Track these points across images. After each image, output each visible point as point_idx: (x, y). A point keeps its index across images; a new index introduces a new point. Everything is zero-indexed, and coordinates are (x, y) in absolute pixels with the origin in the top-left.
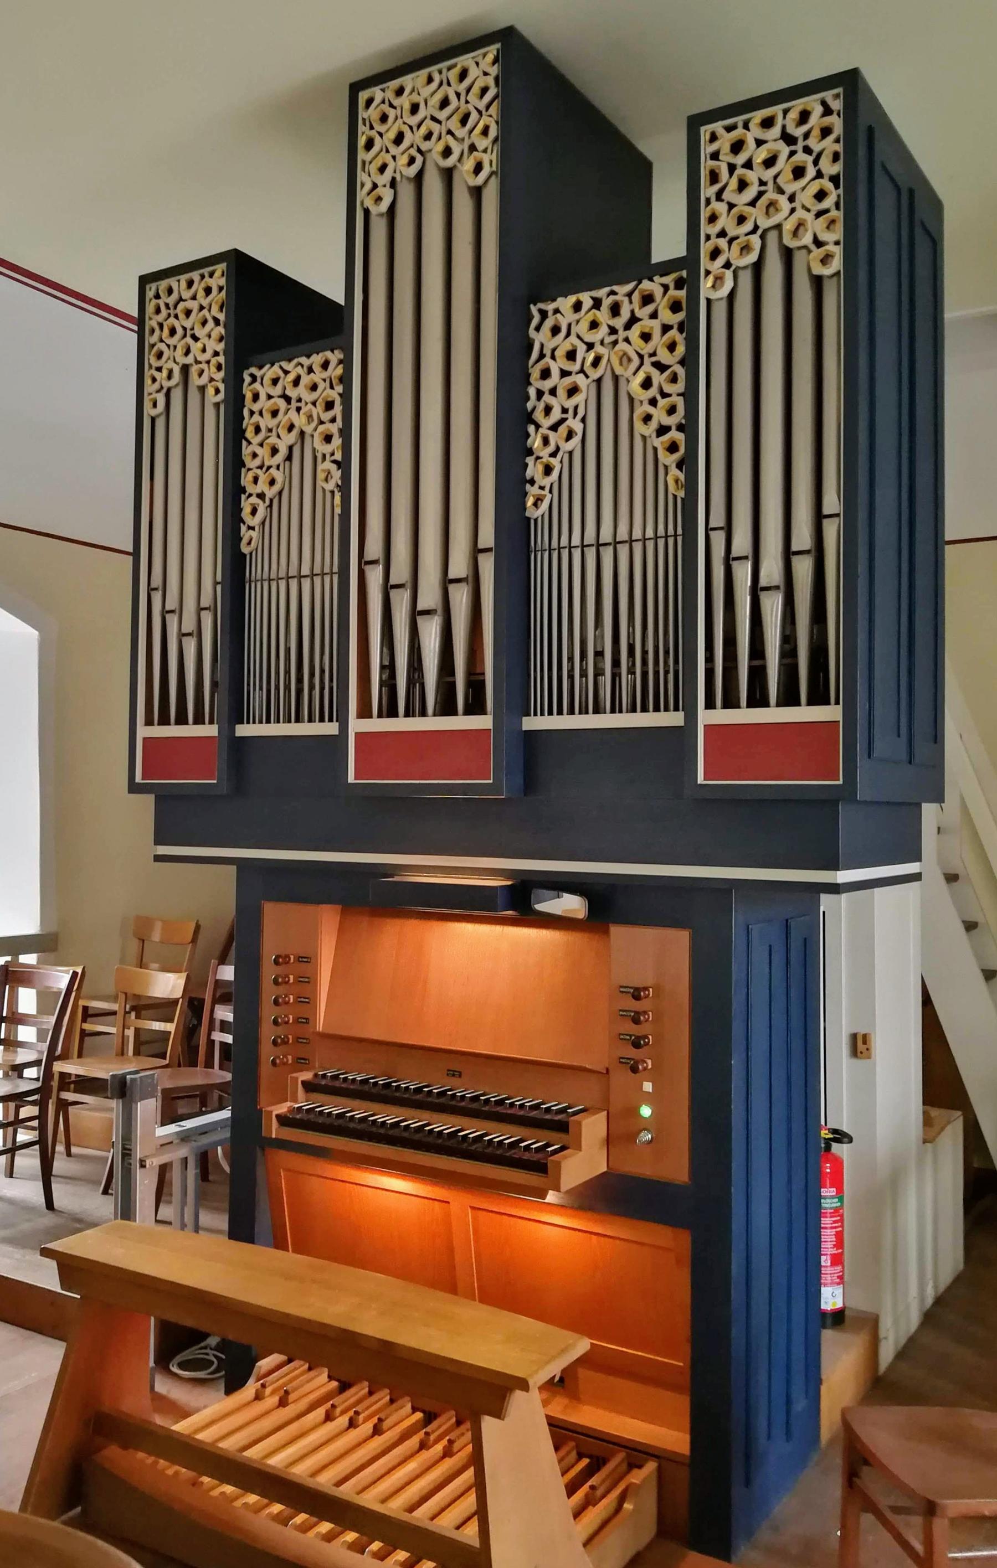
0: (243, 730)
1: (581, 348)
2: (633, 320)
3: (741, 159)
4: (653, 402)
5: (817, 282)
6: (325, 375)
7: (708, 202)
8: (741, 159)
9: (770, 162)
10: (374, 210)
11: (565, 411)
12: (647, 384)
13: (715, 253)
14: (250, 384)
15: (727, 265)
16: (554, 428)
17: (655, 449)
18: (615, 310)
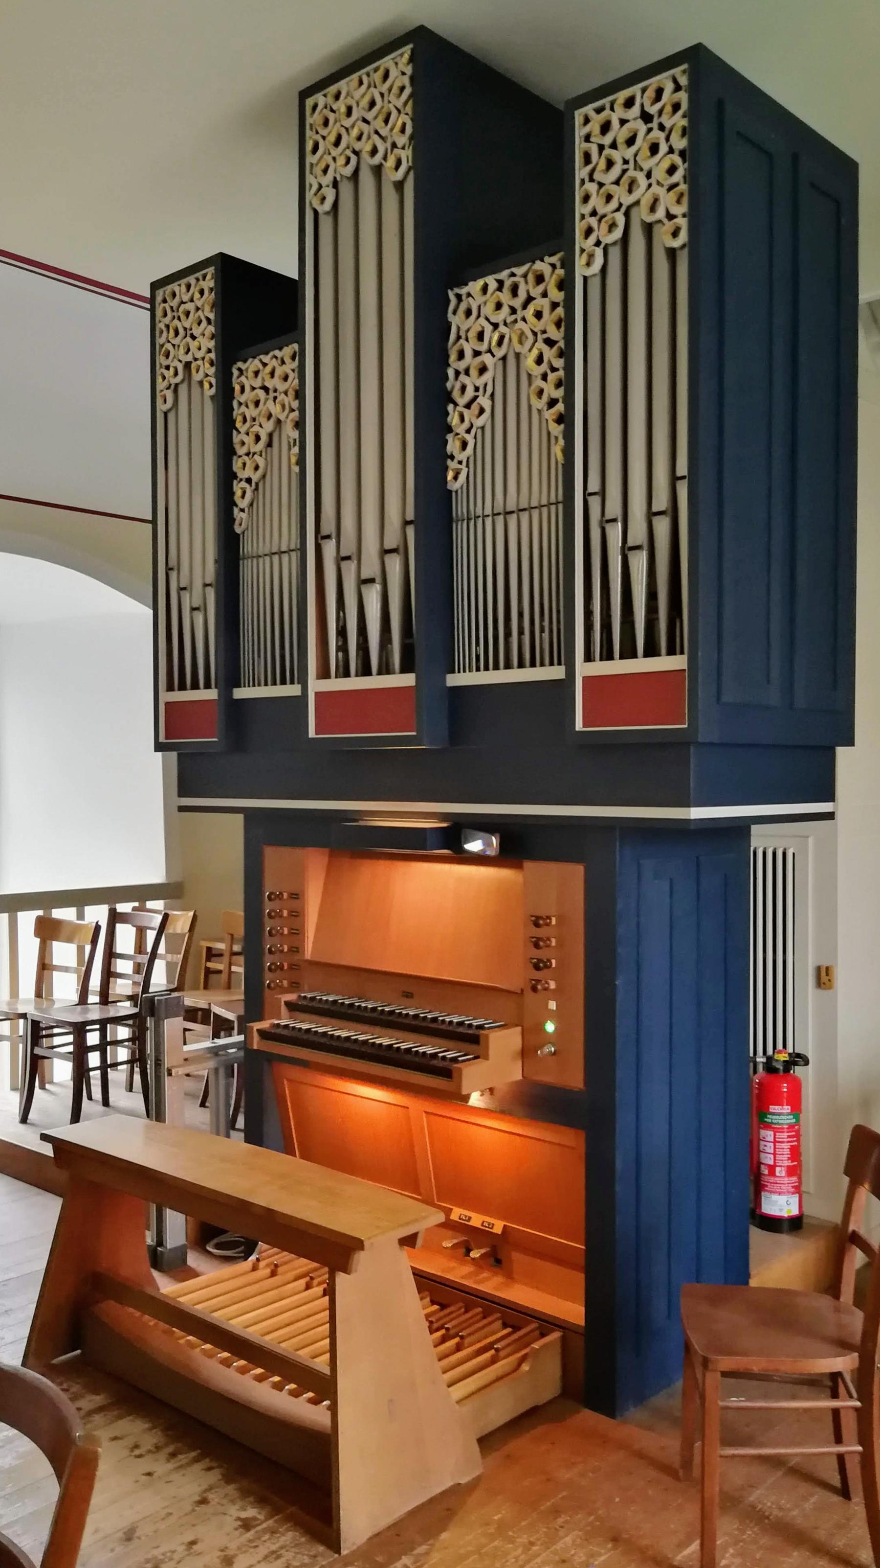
0: (240, 693)
1: (489, 328)
2: (530, 299)
3: (607, 140)
5: (672, 254)
7: (583, 182)
8: (607, 140)
9: (630, 142)
10: (320, 209)
12: (539, 361)
13: (589, 231)
14: (238, 377)
15: (598, 243)
16: (468, 406)
17: (547, 420)
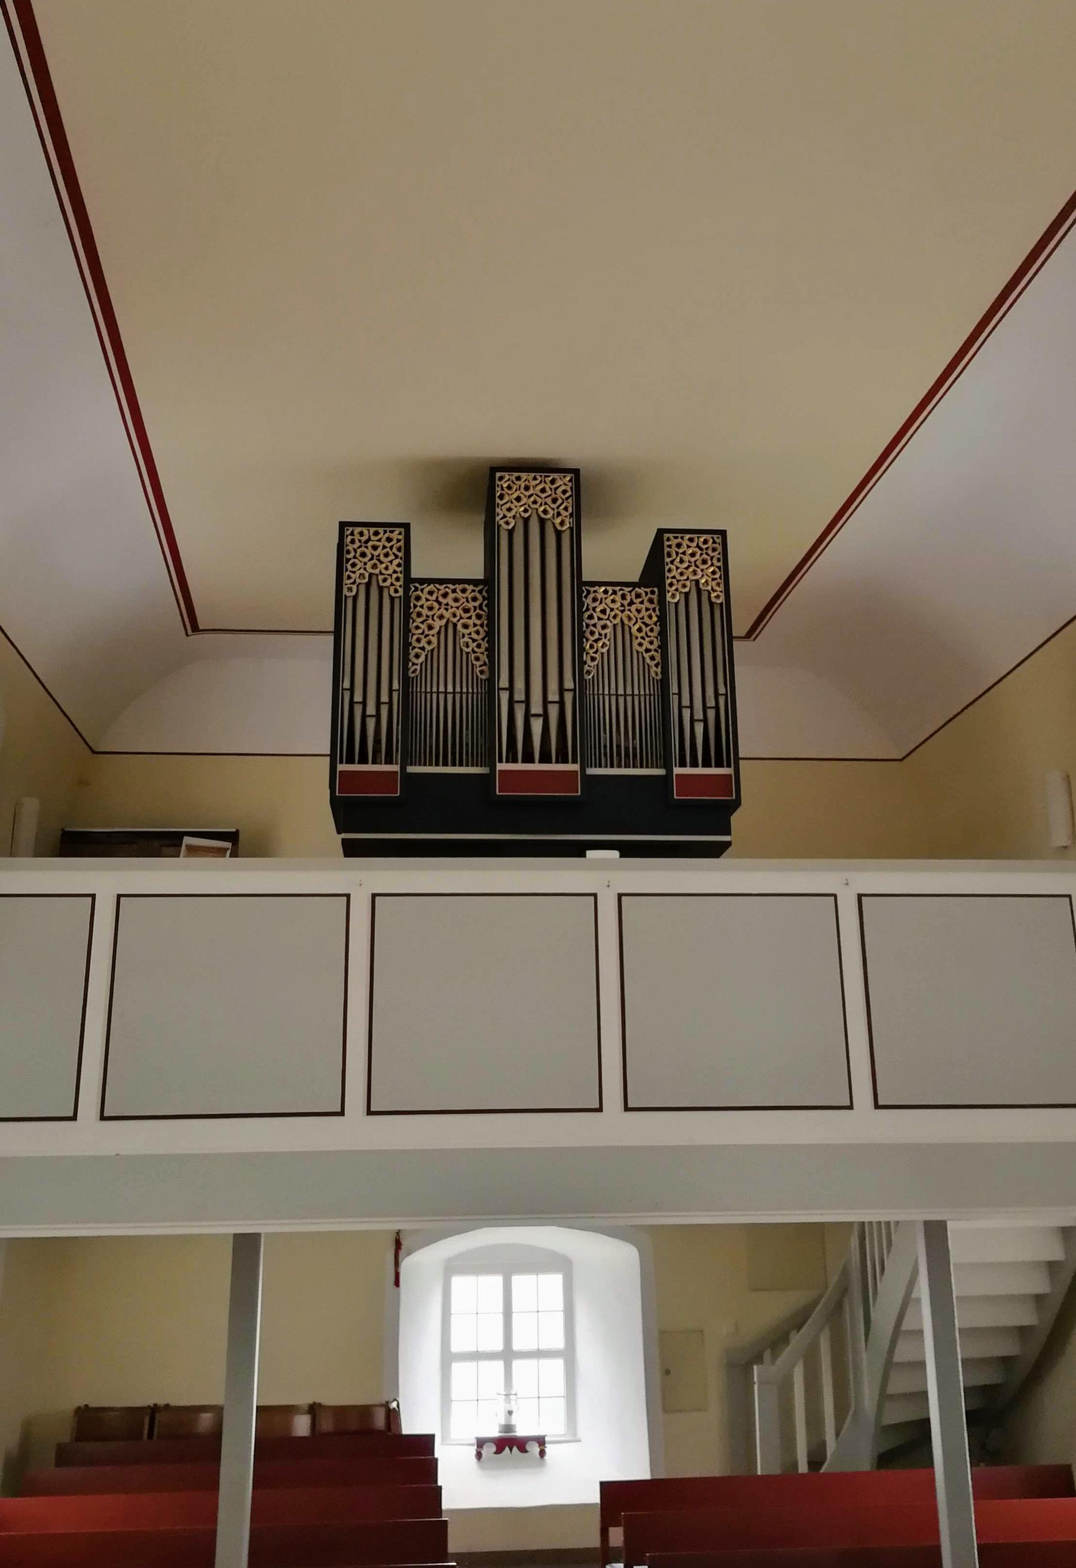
2: (631, 603)
3: (681, 551)
4: (643, 638)
6: (464, 595)
8: (681, 551)
9: (693, 555)
11: (600, 634)
12: (640, 630)
13: (671, 585)
15: (677, 590)
16: (596, 641)
17: (644, 658)
18: (623, 597)
